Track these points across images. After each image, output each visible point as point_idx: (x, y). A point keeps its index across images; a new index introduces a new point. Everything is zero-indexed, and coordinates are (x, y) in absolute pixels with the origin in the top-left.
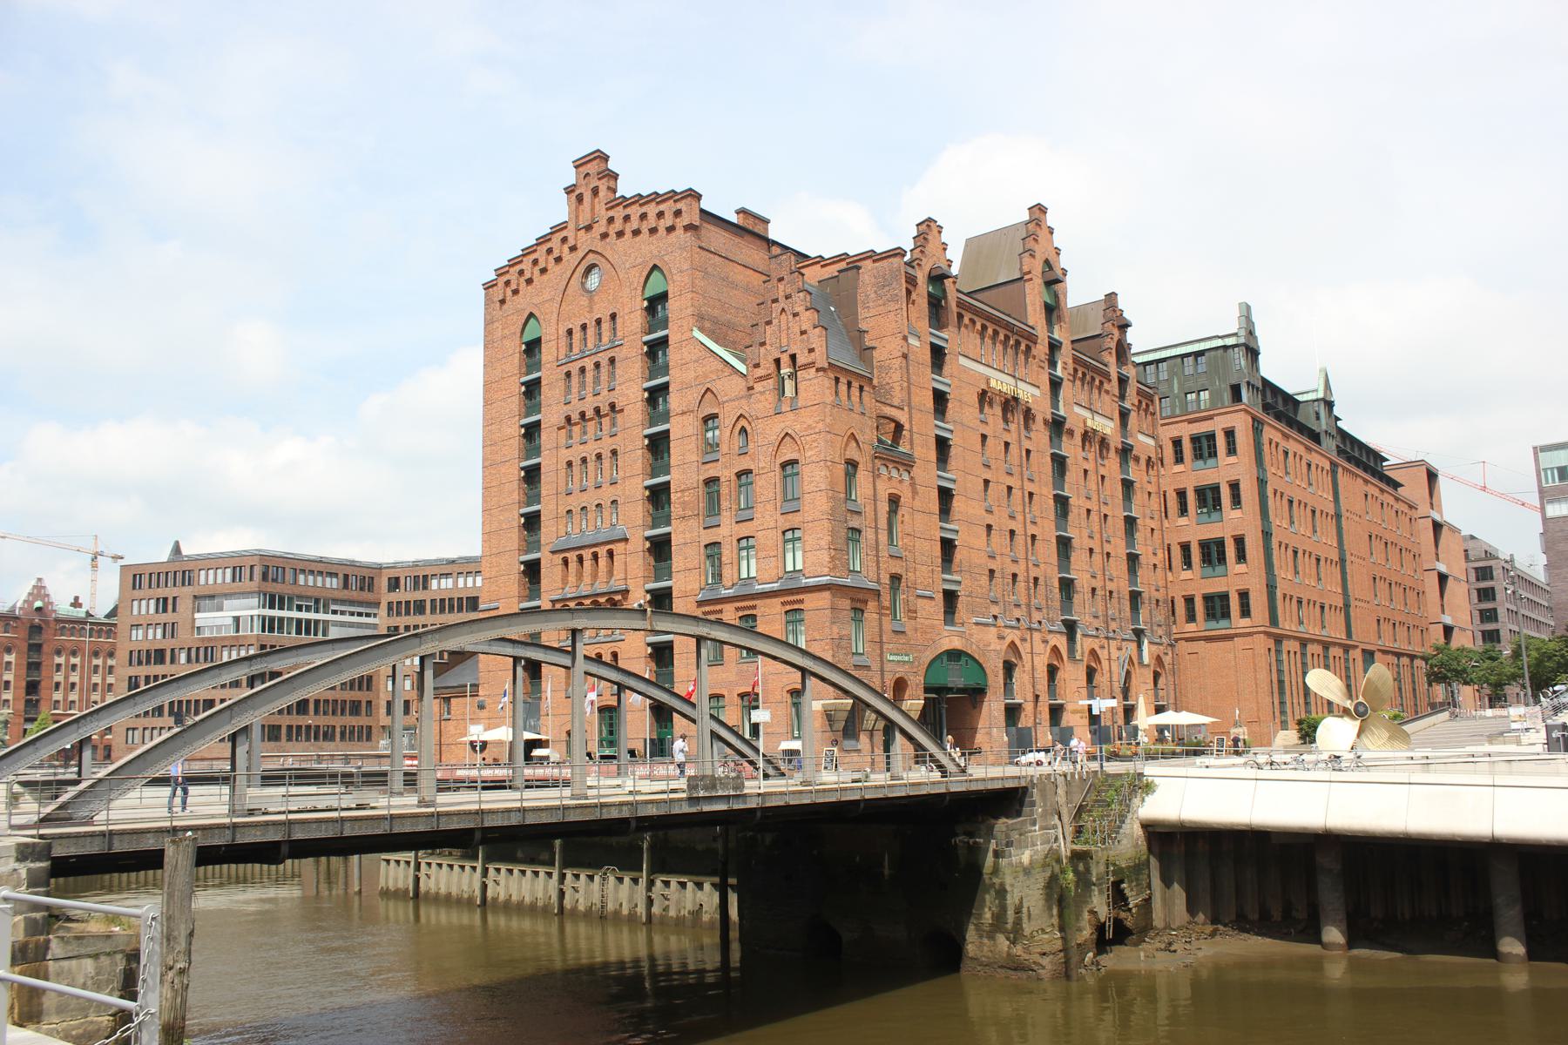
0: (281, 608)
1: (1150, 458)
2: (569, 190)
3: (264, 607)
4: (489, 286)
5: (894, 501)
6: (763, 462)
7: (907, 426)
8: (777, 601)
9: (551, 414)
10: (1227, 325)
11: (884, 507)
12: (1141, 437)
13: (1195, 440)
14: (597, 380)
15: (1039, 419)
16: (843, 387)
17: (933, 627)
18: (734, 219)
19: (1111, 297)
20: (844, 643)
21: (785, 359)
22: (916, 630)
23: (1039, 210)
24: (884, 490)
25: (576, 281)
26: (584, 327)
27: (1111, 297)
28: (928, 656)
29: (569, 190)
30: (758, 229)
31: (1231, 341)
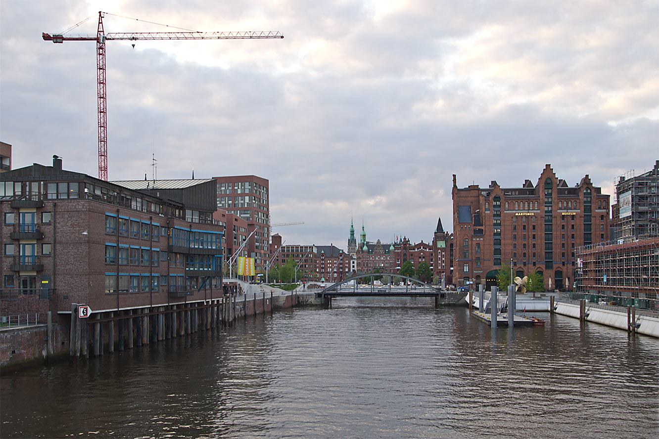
1: (602, 216)
15: (539, 217)
19: (587, 176)
28: (488, 271)
30: (476, 188)
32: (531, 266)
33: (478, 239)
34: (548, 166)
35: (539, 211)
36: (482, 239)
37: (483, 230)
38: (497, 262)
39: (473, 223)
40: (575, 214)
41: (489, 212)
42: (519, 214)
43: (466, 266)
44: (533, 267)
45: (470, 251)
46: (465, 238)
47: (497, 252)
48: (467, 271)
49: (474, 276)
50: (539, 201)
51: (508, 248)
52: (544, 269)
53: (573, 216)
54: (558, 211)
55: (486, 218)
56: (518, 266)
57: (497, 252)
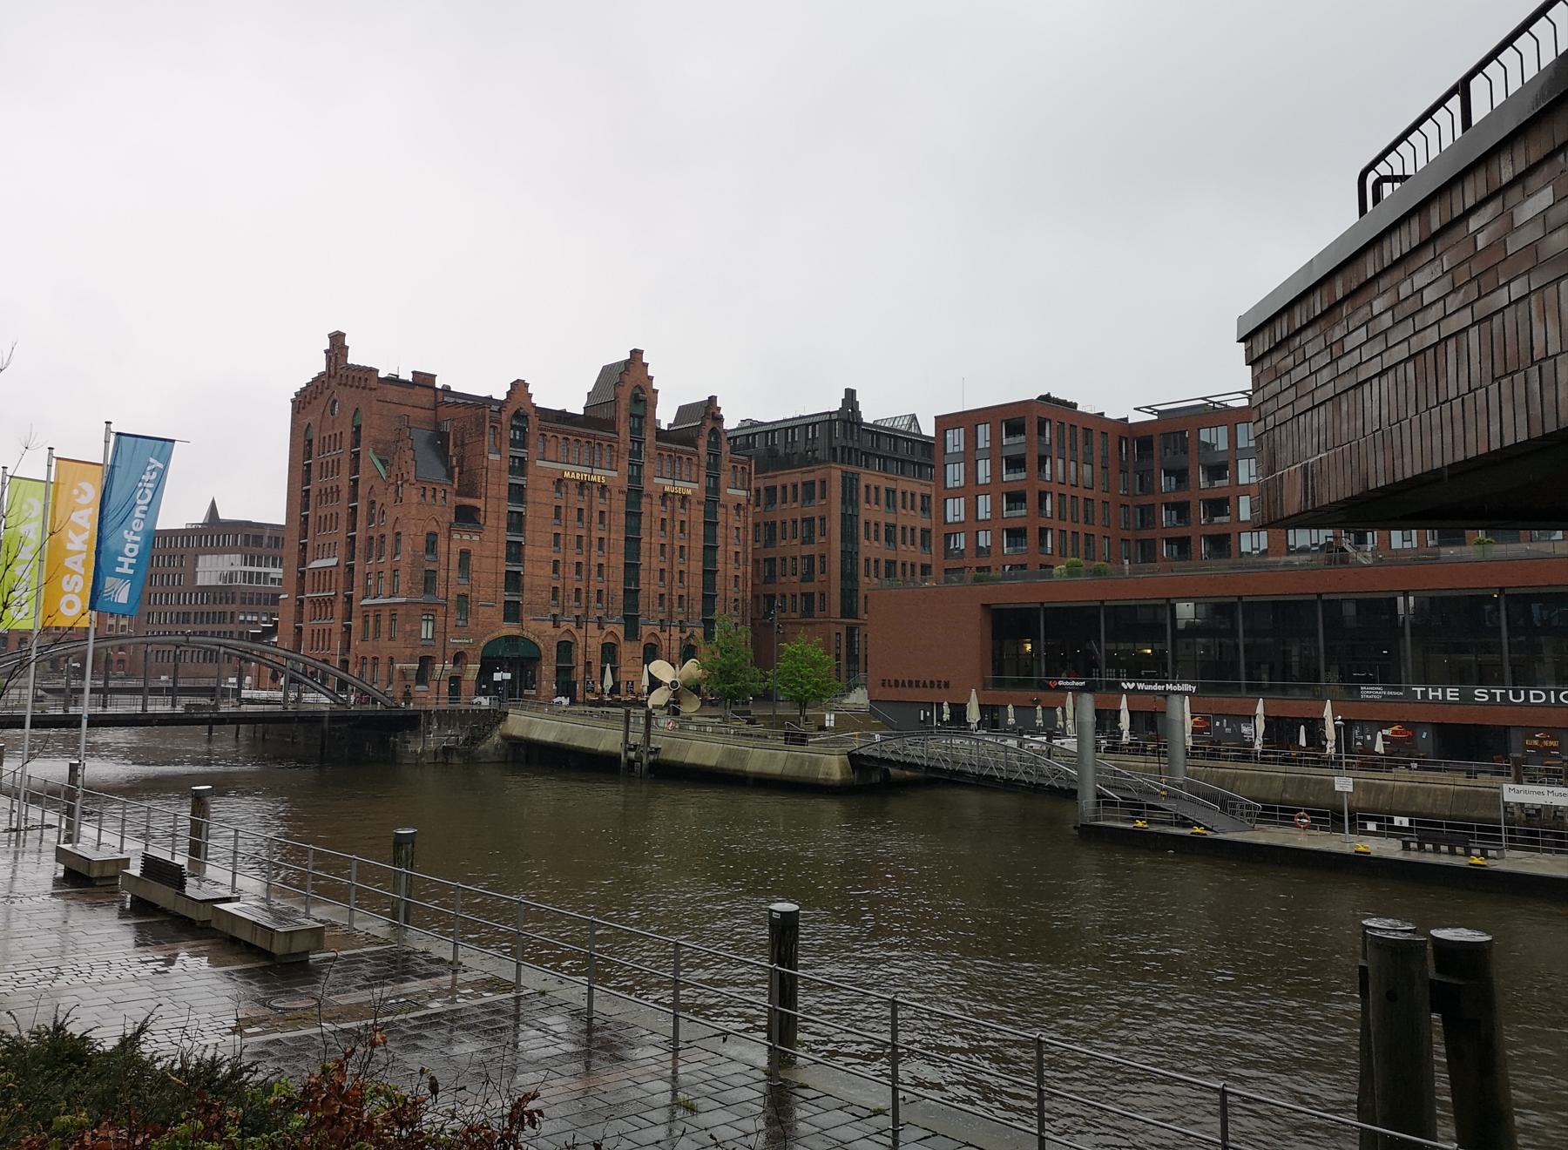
0: (259, 565)
2: (326, 352)
3: (245, 565)
4: (293, 401)
5: (465, 555)
6: (388, 532)
7: (483, 509)
8: (388, 608)
9: (314, 487)
10: (835, 404)
11: (455, 558)
12: (730, 491)
13: (804, 484)
14: (332, 471)
15: (615, 491)
16: (429, 494)
17: (492, 623)
18: (410, 378)
19: (712, 399)
20: (414, 633)
21: (400, 475)
22: (477, 625)
23: (636, 354)
24: (456, 549)
25: (328, 412)
26: (330, 436)
27: (712, 399)
29: (326, 352)
31: (834, 417)
32: (592, 627)
33: (466, 537)
34: (636, 354)
35: (614, 474)
36: (476, 538)
37: (479, 509)
38: (513, 612)
39: (456, 486)
40: (689, 492)
41: (497, 457)
42: (573, 476)
43: (428, 620)
44: (598, 632)
45: (443, 573)
46: (429, 529)
47: (514, 581)
48: (429, 637)
49: (450, 653)
50: (615, 445)
51: (542, 573)
52: (622, 639)
53: (685, 497)
54: (656, 480)
55: (489, 475)
56: (564, 626)
57: (514, 581)
